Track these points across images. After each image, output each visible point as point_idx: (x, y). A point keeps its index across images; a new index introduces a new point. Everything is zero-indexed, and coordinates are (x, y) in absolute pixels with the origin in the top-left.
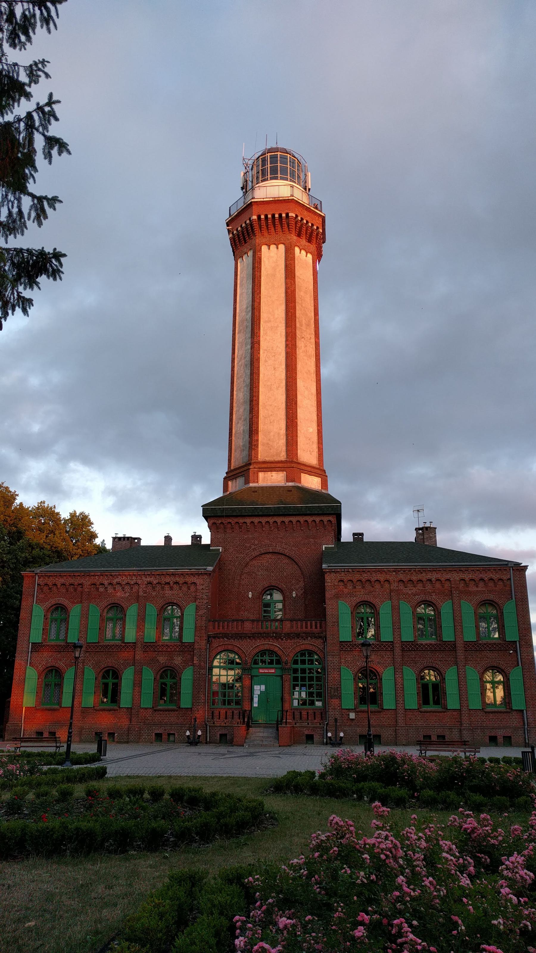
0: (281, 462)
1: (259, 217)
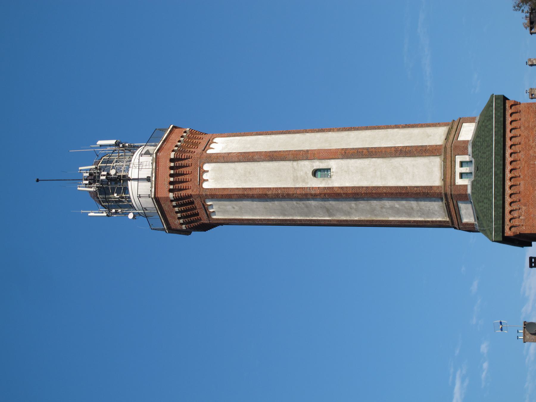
0: (445, 161)
1: (171, 191)
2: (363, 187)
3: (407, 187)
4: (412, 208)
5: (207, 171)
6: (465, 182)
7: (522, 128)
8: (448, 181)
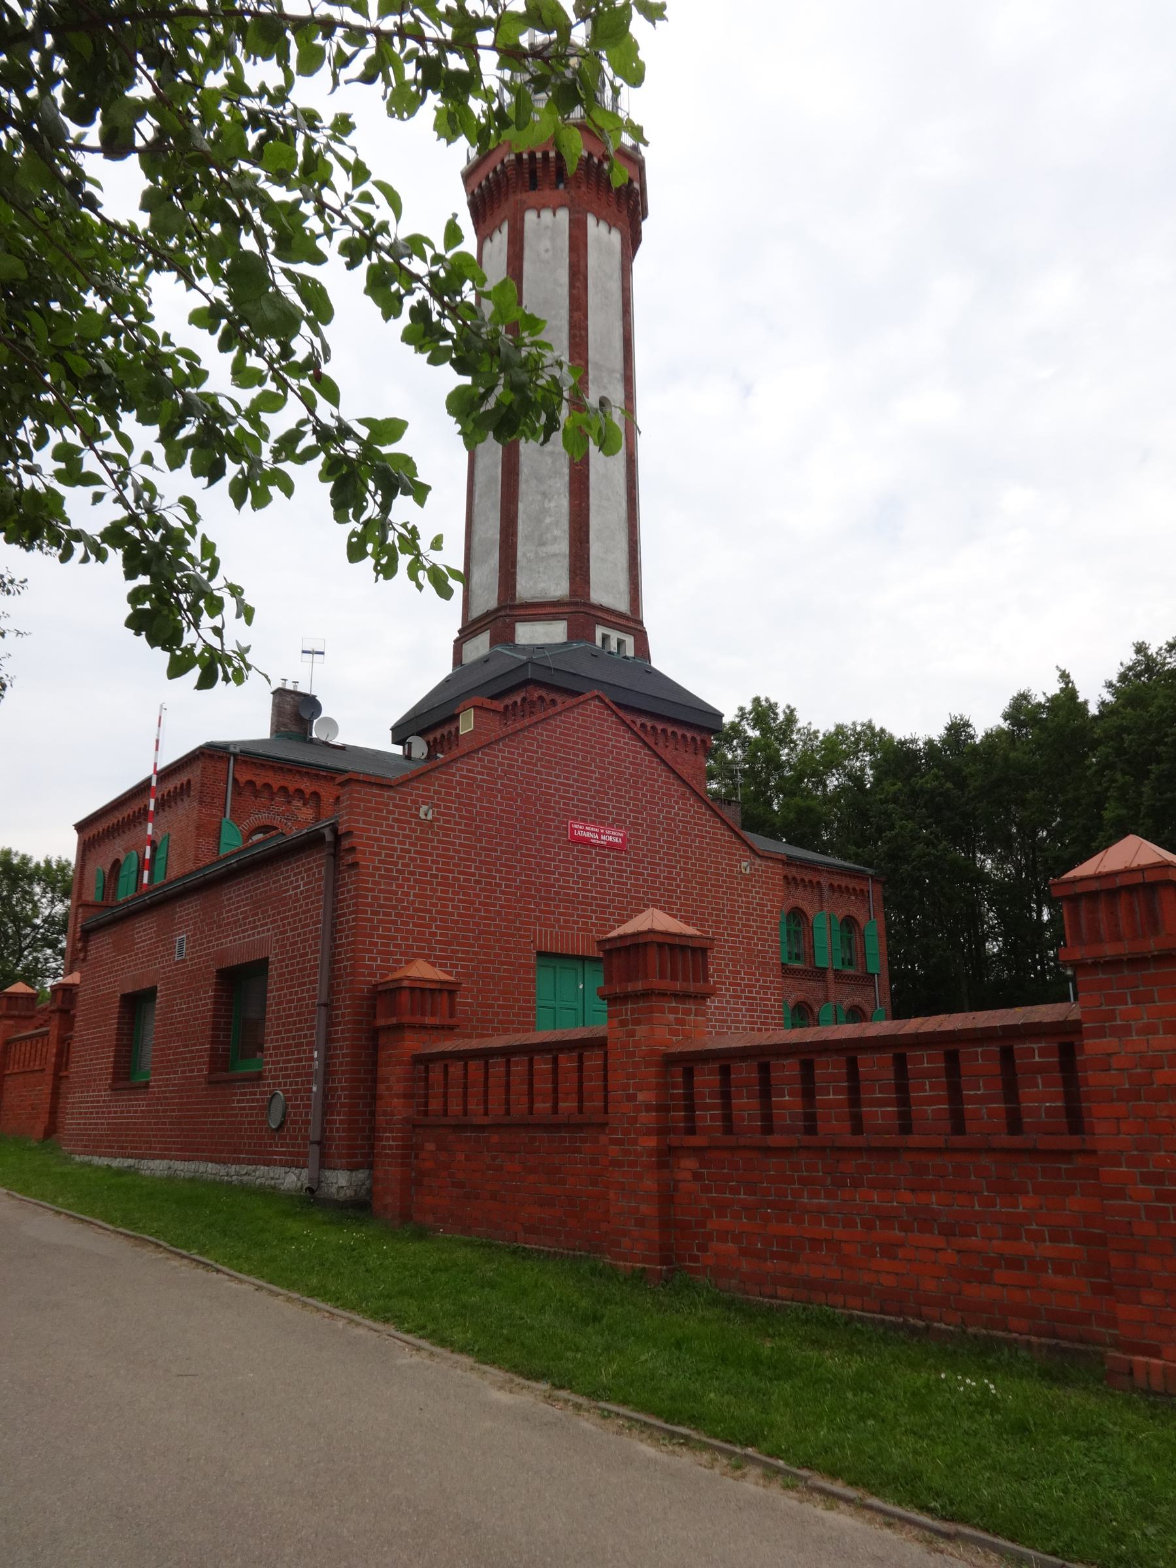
1: (590, 155)
2: (588, 470)
3: (588, 542)
4: (542, 544)
5: (610, 232)
6: (598, 642)
7: (675, 753)
8: (599, 614)
